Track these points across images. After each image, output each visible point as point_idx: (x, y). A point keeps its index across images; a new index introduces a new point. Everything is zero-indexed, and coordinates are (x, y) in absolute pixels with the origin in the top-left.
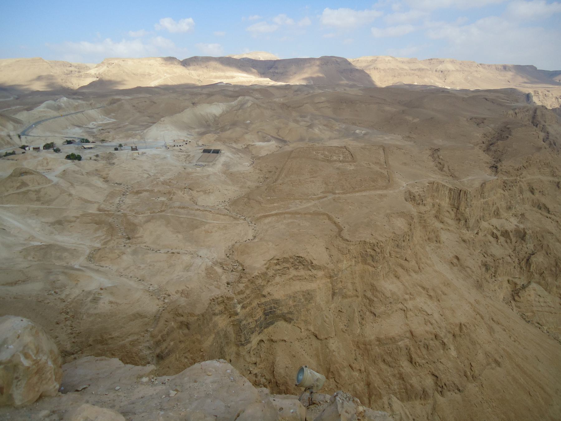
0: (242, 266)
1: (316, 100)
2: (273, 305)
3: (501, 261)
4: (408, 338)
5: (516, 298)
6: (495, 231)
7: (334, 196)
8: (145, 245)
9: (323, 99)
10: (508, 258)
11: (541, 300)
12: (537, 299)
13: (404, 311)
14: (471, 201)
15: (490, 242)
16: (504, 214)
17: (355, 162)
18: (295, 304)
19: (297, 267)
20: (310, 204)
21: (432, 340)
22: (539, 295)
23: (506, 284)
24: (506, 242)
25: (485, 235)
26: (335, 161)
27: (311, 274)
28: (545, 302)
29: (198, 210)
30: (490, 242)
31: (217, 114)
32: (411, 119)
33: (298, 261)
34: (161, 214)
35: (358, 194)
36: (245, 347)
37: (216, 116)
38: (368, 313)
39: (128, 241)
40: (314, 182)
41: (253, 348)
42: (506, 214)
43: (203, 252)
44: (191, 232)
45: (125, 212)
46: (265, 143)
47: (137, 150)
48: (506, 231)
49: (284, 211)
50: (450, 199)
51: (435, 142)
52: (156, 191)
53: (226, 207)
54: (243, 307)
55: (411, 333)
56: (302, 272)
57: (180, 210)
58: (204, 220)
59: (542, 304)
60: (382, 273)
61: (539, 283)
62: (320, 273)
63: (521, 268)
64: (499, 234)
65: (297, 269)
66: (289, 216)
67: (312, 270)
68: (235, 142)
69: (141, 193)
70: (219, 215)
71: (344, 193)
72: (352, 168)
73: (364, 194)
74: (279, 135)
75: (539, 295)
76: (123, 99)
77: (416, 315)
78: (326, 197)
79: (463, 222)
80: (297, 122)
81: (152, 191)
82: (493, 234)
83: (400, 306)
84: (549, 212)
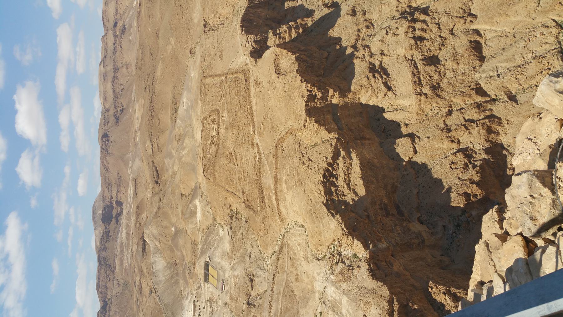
0: (334, 240)
1: (150, 152)
2: (377, 207)
7: (256, 136)
9: (148, 143)
18: (375, 182)
29: (272, 289)
32: (170, 47)
35: (254, 109)
36: (426, 238)
37: (166, 267)
41: (427, 229)
43: (319, 286)
46: (198, 210)
49: (273, 192)
53: (270, 256)
54: (380, 241)
57: (273, 311)
70: (279, 265)
71: (253, 125)
72: (225, 114)
73: (254, 103)
74: (189, 195)
78: (257, 144)
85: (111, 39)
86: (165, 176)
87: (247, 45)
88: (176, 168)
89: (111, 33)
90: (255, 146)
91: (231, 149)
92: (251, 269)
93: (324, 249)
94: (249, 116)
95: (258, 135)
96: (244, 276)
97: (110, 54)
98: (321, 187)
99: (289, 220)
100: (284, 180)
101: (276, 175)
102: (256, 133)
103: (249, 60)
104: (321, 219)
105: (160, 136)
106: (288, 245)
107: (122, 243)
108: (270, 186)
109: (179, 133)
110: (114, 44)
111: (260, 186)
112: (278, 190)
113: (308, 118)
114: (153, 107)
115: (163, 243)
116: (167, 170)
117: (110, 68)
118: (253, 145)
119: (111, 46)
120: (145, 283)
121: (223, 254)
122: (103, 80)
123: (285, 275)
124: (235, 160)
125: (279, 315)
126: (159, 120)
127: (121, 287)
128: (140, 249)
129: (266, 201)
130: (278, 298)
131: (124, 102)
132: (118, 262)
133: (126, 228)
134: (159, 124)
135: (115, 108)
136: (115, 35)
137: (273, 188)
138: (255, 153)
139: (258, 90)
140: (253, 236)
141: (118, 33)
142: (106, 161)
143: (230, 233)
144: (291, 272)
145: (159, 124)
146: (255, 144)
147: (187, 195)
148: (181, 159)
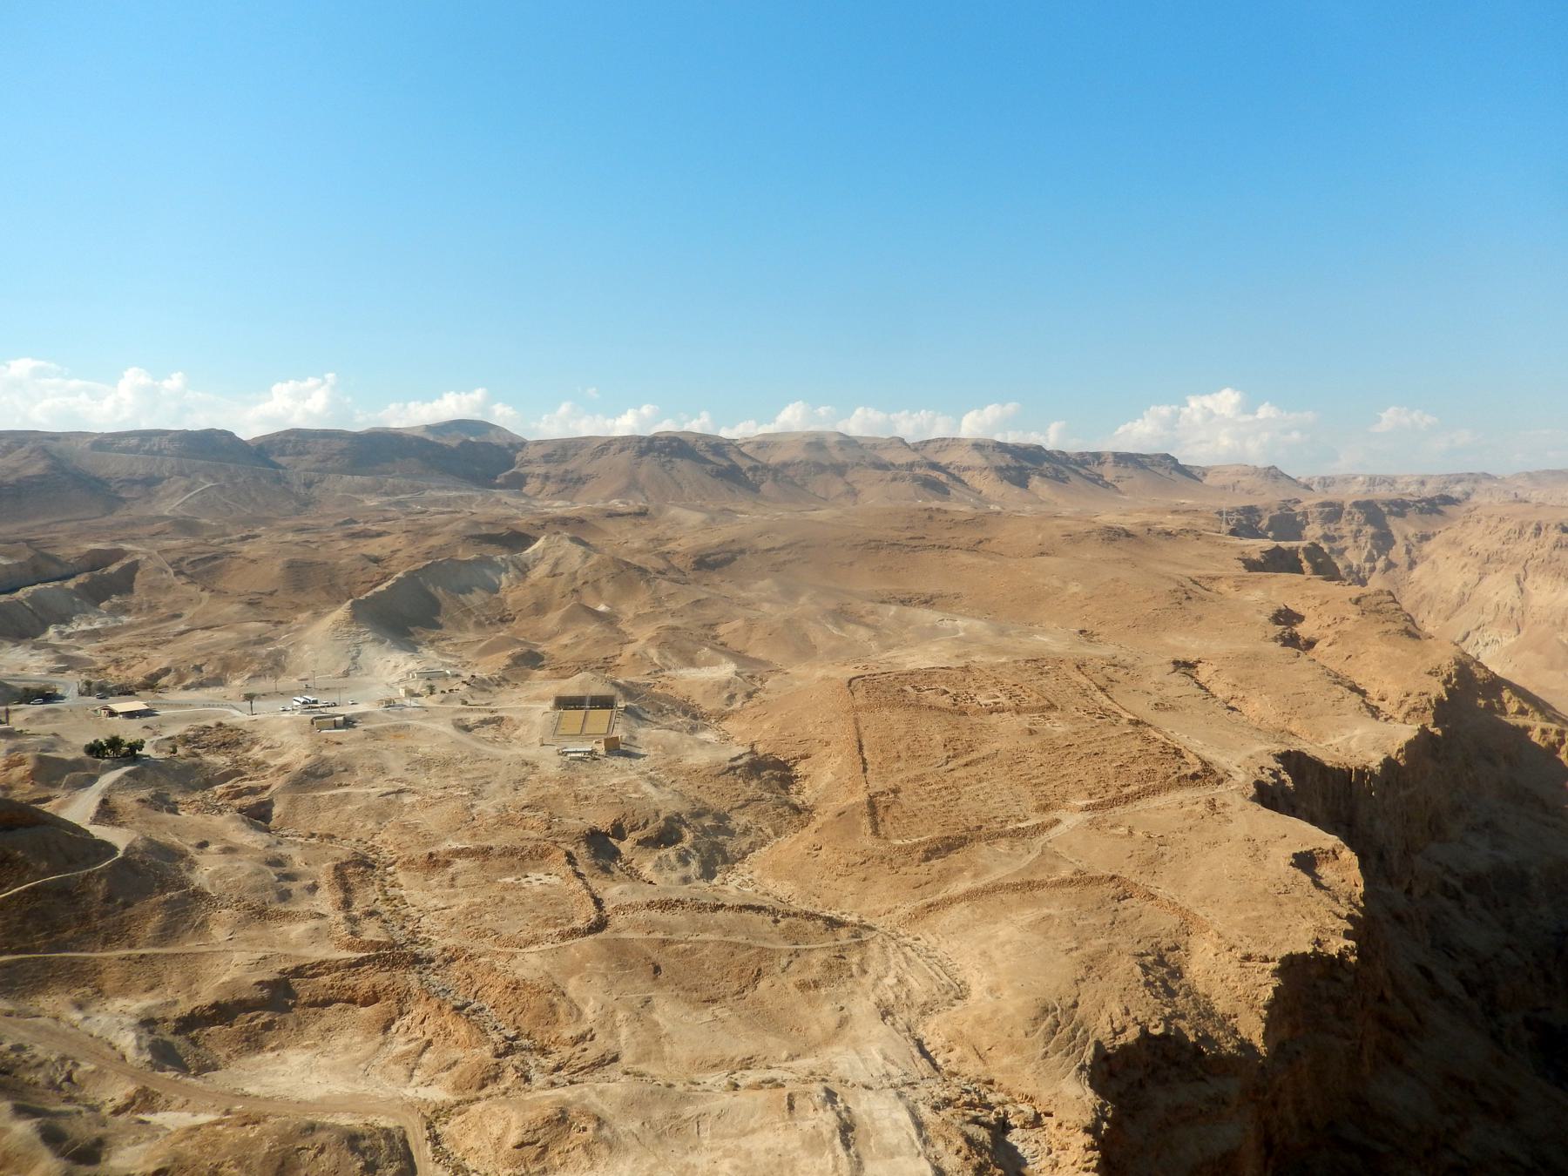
1: (763, 544)
6: (1451, 881)
7: (1080, 817)
9: (780, 541)
10: (1507, 952)
15: (1447, 914)
25: (1427, 894)
30: (1447, 914)
32: (1056, 583)
34: (600, 936)
35: (1141, 804)
45: (449, 942)
46: (705, 669)
49: (980, 884)
51: (1171, 641)
52: (497, 851)
57: (655, 914)
64: (1459, 885)
69: (448, 863)
70: (793, 920)
76: (136, 552)
78: (1058, 821)
80: (747, 604)
81: (485, 852)
82: (1445, 889)
85: (907, 457)
86: (721, 585)
87: (1267, 772)
88: (766, 607)
89: (915, 457)
90: (1048, 817)
91: (985, 750)
92: (688, 836)
93: (972, 1068)
94: (1112, 793)
95: (1091, 822)
96: (662, 816)
98: (1132, 1034)
99: (933, 940)
100: (1046, 911)
101: (1042, 885)
102: (1088, 815)
107: (420, 490)
108: (987, 870)
113: (1276, 965)
114: (877, 547)
115: (552, 586)
116: (742, 587)
117: (839, 457)
118: (1045, 808)
119: (887, 457)
120: (398, 546)
121: (668, 749)
124: (962, 761)
125: (660, 935)
126: (851, 564)
127: (302, 491)
128: (484, 530)
129: (937, 864)
130: (705, 929)
135: (750, 469)
136: (911, 466)
140: (769, 831)
141: (918, 471)
142: (622, 450)
143: (740, 762)
144: (808, 965)
146: (1052, 815)
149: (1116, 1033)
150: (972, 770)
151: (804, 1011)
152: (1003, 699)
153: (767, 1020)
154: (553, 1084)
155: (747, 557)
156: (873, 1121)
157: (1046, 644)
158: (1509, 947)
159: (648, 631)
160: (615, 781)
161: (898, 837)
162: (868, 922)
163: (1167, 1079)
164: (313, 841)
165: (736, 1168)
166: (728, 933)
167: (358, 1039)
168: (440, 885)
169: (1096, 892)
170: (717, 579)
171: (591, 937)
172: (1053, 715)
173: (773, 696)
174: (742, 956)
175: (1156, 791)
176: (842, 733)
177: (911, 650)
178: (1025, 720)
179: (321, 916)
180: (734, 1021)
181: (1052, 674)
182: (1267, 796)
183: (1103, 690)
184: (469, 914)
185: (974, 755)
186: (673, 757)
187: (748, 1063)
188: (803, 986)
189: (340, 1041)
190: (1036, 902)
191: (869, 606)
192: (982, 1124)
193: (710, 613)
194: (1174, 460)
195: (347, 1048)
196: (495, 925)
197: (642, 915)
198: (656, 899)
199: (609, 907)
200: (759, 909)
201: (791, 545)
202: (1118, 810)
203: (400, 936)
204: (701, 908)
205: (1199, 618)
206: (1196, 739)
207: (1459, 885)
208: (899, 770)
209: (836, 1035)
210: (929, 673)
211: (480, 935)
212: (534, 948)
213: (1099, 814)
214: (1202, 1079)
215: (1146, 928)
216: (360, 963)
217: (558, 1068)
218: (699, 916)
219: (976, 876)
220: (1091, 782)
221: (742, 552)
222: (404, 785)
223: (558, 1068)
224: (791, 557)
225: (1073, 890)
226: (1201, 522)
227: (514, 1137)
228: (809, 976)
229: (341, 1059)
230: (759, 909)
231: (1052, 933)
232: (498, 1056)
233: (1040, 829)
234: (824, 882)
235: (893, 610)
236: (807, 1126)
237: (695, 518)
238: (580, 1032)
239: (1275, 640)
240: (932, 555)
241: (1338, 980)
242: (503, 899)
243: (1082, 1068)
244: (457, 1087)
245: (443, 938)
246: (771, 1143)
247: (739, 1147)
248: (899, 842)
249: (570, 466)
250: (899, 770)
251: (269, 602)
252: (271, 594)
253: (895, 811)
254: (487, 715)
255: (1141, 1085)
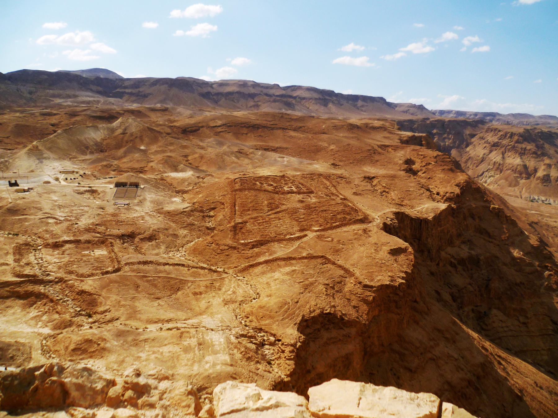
0: (274, 335)
1: (212, 124)
3: (464, 291)
4: (447, 390)
5: (484, 327)
6: (452, 260)
7: (315, 234)
8: (119, 322)
9: (219, 123)
10: (469, 286)
11: (504, 325)
12: (500, 325)
13: (434, 360)
14: (432, 230)
15: (450, 272)
16: (457, 242)
17: (312, 192)
19: (327, 326)
20: (295, 247)
21: (467, 387)
22: (501, 321)
23: (472, 315)
24: (464, 270)
26: (289, 193)
27: (345, 333)
28: (507, 327)
31: (98, 140)
32: (326, 145)
33: (327, 319)
35: (339, 230)
38: (402, 370)
39: (90, 320)
40: (280, 219)
42: (458, 242)
44: (173, 296)
45: (59, 275)
47: (18, 185)
48: (463, 259)
49: (271, 258)
50: (411, 229)
51: (365, 169)
52: (83, 241)
55: (449, 383)
56: (334, 333)
57: (141, 266)
58: (182, 278)
59: (505, 329)
60: (405, 321)
61: (499, 309)
62: (353, 331)
63: (482, 295)
64: (456, 262)
65: (328, 329)
66: (283, 263)
67: (344, 328)
68: (141, 172)
69: (62, 246)
70: (196, 270)
72: (314, 200)
74: (190, 164)
75: (501, 321)
77: (447, 363)
78: (306, 235)
79: (426, 253)
80: (202, 148)
81: (77, 242)
83: (429, 355)
84: (490, 236)
87: (389, 219)
88: (210, 150)
90: (302, 234)
91: (284, 207)
94: (329, 225)
95: (318, 236)
97: (265, 91)
98: (318, 311)
100: (294, 268)
101: (294, 259)
102: (318, 233)
103: (378, 221)
104: (288, 317)
105: (230, 134)
106: (223, 279)
108: (275, 252)
109: (248, 153)
110: (274, 95)
111: (268, 242)
112: (279, 263)
114: (258, 128)
115: (123, 138)
116: (201, 141)
117: (252, 91)
118: (302, 230)
119: (271, 92)
122: (240, 83)
123: (192, 279)
124: (273, 212)
126: (246, 134)
127: (28, 96)
129: (256, 250)
131: (223, 101)
132: (56, 92)
133: (94, 101)
134: (243, 134)
136: (282, 96)
137: (275, 256)
138: (294, 234)
139: (360, 232)
143: (187, 210)
145: (243, 134)
147: (190, 162)
148: (225, 155)
149: (311, 312)
150: (277, 215)
151: (194, 302)
152: (294, 189)
153: (179, 306)
154: (91, 328)
155: (205, 129)
156: (212, 342)
157: (317, 168)
158: (470, 284)
159: (160, 157)
160: (135, 215)
161: (243, 240)
162: (226, 271)
163: (329, 328)
164: (10, 236)
165: (156, 358)
166: (169, 274)
167: (19, 311)
168: (58, 254)
169: (314, 262)
170: (191, 137)
171: (114, 274)
172: (312, 195)
173: (205, 185)
174: (173, 282)
175: (345, 225)
176: (228, 200)
177: (264, 169)
178: (300, 197)
179: (7, 264)
180: (166, 306)
181: (316, 180)
182: (387, 228)
183: (334, 186)
184: (66, 265)
185: (278, 210)
186: (160, 207)
187: (169, 321)
188: (195, 294)
189: (11, 311)
190: (291, 265)
191: (251, 150)
192: (254, 343)
193: (187, 151)
194: (384, 100)
195: (14, 313)
196: (77, 269)
197: (135, 267)
198: (141, 260)
199: (123, 263)
200: (183, 265)
201: (223, 125)
202: (330, 232)
203: (38, 272)
204: (159, 264)
205: (377, 161)
206: (363, 204)
207: (456, 262)
208: (249, 215)
209: (204, 312)
210: (267, 178)
211: (71, 273)
212: (92, 278)
213: (323, 233)
214: (342, 328)
215: (331, 275)
216: (22, 282)
217: (94, 322)
218: (158, 267)
219: (270, 255)
220: (321, 220)
221: (202, 127)
222: (49, 215)
223: (94, 322)
224: (223, 130)
225: (306, 261)
226: (387, 124)
227: (72, 347)
228: (197, 291)
229: (11, 318)
230: (183, 265)
231: (294, 276)
232: (72, 317)
233: (299, 238)
234: (212, 256)
235: (260, 153)
236: (185, 343)
237: (188, 112)
238: (105, 309)
239: (404, 170)
240: (279, 132)
241: (398, 295)
242: (82, 259)
243: (295, 324)
244: (55, 328)
245: (56, 274)
246: (171, 349)
247: (159, 351)
248: (243, 242)
249: (141, 90)
250: (249, 215)
251: (6, 141)
252: (8, 138)
253: (243, 231)
254: (88, 189)
255: (319, 331)
